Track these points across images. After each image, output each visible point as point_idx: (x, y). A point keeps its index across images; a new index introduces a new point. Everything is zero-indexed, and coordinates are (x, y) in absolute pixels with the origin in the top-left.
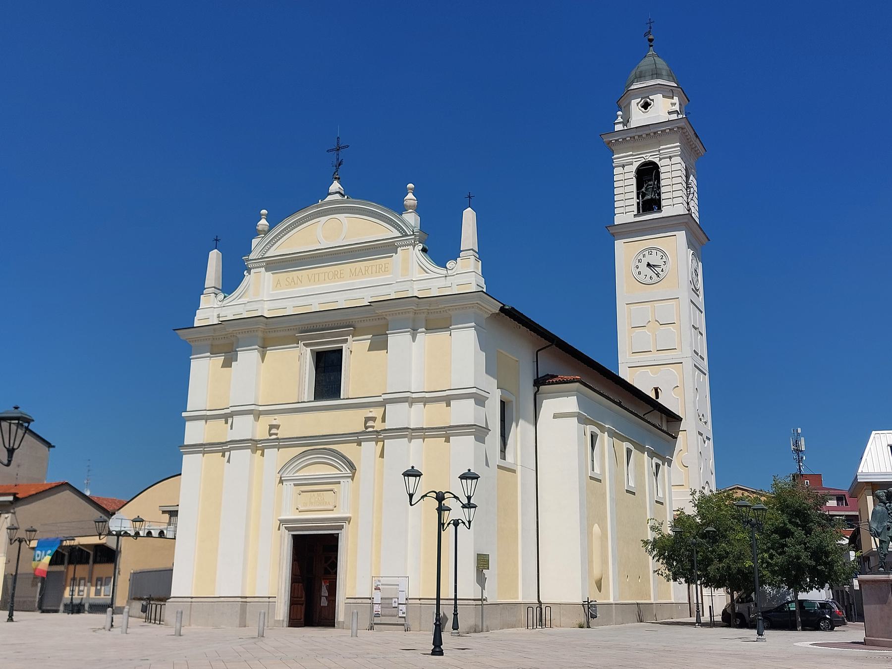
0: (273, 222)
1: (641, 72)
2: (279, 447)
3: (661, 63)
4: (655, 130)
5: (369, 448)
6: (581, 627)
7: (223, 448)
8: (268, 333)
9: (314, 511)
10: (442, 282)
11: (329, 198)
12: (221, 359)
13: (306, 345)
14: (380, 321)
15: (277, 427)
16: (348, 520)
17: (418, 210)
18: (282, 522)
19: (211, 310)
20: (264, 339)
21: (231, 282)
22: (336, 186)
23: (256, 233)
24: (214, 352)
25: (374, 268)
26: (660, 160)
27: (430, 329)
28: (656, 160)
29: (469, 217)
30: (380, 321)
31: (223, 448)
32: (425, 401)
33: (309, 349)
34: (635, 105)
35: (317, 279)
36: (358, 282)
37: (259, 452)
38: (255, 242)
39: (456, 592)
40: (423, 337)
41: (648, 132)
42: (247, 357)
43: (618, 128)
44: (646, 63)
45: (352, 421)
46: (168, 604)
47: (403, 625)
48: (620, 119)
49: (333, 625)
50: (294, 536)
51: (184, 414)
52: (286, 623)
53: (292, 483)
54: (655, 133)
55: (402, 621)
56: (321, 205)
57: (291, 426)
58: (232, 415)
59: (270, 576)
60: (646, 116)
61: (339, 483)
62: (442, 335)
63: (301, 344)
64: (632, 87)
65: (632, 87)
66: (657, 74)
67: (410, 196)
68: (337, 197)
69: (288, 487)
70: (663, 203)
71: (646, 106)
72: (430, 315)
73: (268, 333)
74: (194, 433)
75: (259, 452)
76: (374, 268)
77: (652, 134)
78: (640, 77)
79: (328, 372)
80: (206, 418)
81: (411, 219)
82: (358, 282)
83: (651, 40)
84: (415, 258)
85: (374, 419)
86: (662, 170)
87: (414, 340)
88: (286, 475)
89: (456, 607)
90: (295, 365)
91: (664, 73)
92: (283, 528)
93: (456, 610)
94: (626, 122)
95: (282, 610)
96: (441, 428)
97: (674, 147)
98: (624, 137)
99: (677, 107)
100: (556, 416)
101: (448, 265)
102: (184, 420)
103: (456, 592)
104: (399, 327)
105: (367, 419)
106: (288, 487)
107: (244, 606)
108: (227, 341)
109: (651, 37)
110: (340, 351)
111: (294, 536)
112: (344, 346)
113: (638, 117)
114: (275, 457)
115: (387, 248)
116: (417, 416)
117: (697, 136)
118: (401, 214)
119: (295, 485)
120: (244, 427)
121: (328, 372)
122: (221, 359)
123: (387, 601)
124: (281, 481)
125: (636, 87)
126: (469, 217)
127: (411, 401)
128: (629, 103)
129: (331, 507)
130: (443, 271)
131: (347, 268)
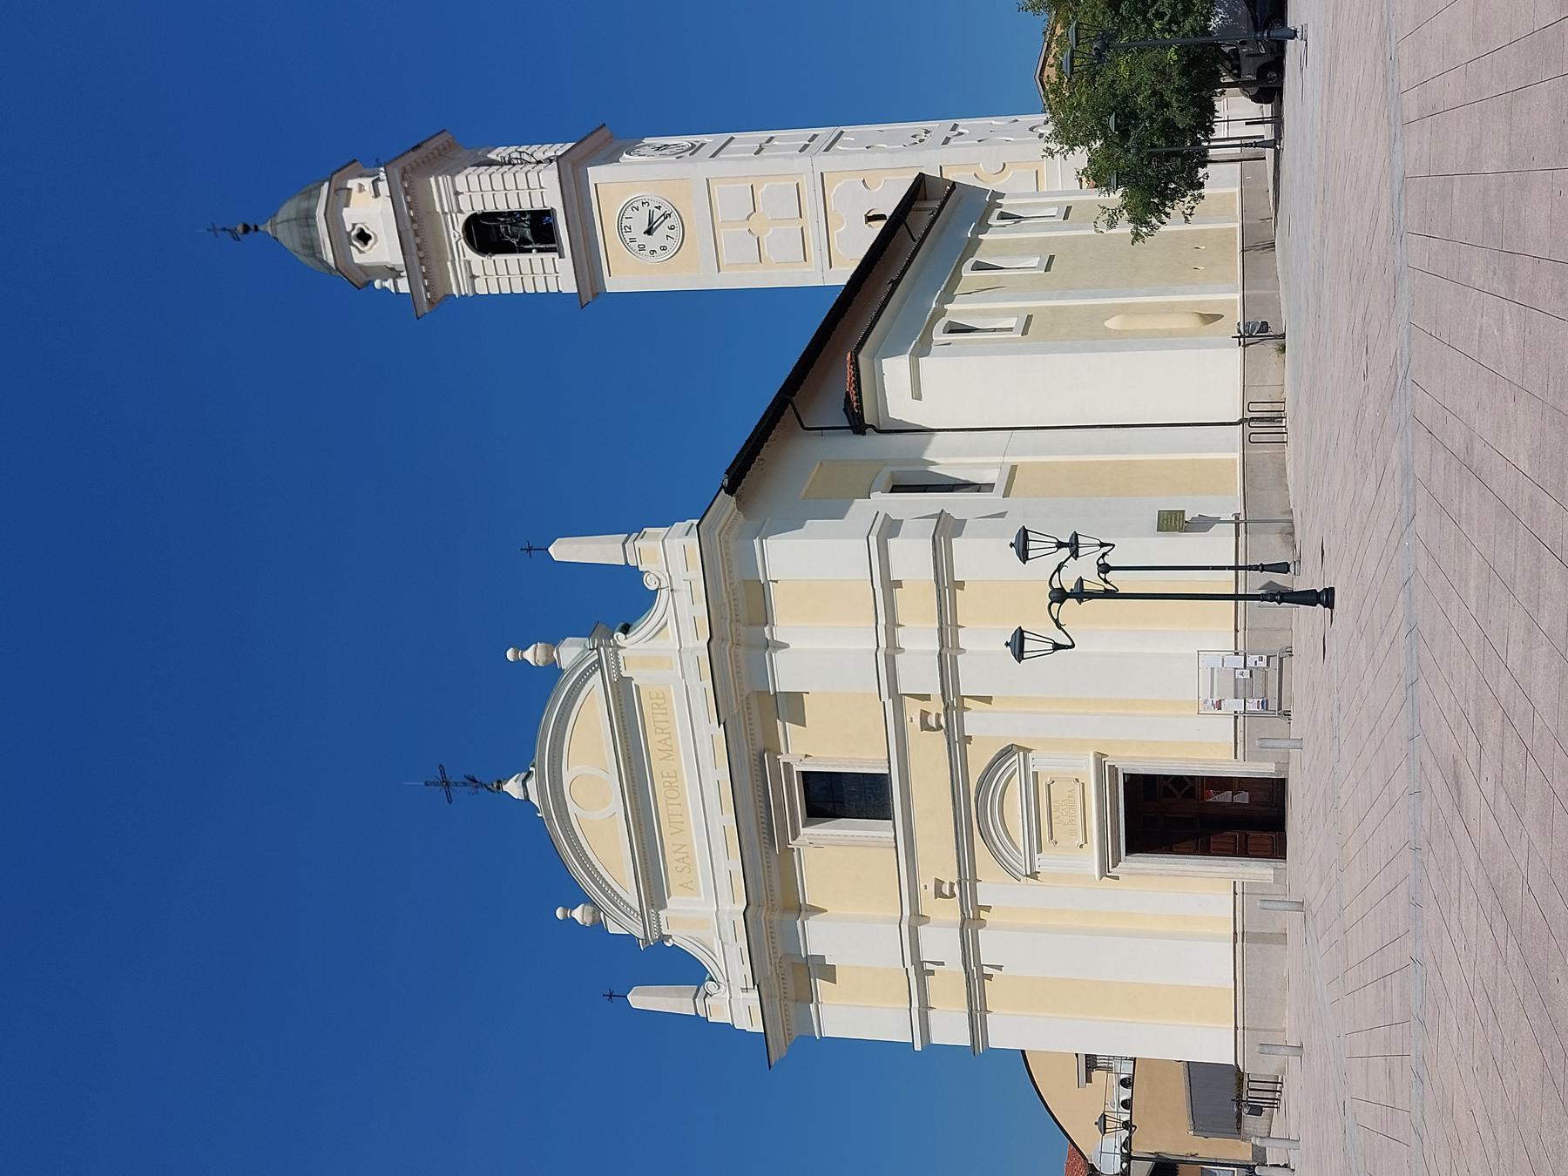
0: (579, 896)
1: (304, 246)
3: (289, 210)
4: (408, 221)
5: (975, 721)
6: (1283, 349)
7: (976, 977)
8: (774, 903)
9: (1085, 817)
10: (683, 597)
11: (534, 798)
12: (821, 985)
13: (795, 835)
14: (752, 707)
15: (939, 884)
16: (1100, 758)
17: (554, 641)
18: (1104, 872)
19: (734, 1003)
20: (785, 909)
21: (684, 969)
22: (512, 788)
23: (598, 927)
24: (808, 996)
25: (659, 718)
26: (460, 211)
27: (766, 618)
28: (462, 218)
29: (565, 550)
30: (752, 707)
31: (976, 977)
32: (893, 624)
33: (803, 831)
34: (363, 256)
35: (679, 819)
36: (683, 745)
37: (983, 914)
38: (613, 929)
39: (1223, 568)
40: (781, 630)
41: (411, 233)
42: (818, 938)
43: (404, 286)
44: (288, 237)
45: (929, 752)
46: (1247, 1069)
47: (1281, 659)
48: (389, 284)
49: (1282, 783)
50: (1128, 852)
51: (918, 1047)
52: (1280, 864)
54: (413, 221)
55: (1275, 662)
56: (547, 812)
57: (937, 860)
58: (918, 963)
59: (1197, 893)
60: (382, 236)
61: (1036, 774)
62: (776, 593)
63: (793, 844)
64: (331, 261)
65: (331, 261)
66: (307, 219)
67: (528, 655)
68: (532, 784)
69: (1042, 862)
70: (538, 206)
71: (364, 237)
72: (741, 616)
73: (774, 903)
74: (950, 1029)
75: (983, 914)
76: (659, 718)
77: (416, 228)
78: (313, 248)
79: (842, 796)
80: (925, 1008)
81: (569, 653)
82: (683, 745)
83: (246, 229)
84: (640, 645)
85: (924, 715)
86: (479, 208)
87: (786, 646)
88: (1023, 868)
89: (1250, 568)
90: (830, 853)
91: (304, 205)
92: (1114, 872)
93: (1256, 568)
94: (394, 273)
95: (1256, 871)
96: (939, 597)
97: (439, 187)
98: (420, 276)
99: (367, 182)
100: (917, 396)
101: (652, 587)
102: (929, 1047)
103: (1223, 568)
104: (762, 672)
105: (925, 726)
106: (1042, 862)
108: (789, 973)
109: (240, 228)
110: (806, 776)
111: (1128, 852)
112: (796, 769)
113: (385, 250)
114: (992, 887)
115: (623, 696)
116: (919, 640)
117: (418, 146)
118: (562, 671)
120: (941, 942)
121: (842, 796)
122: (821, 985)
123: (1240, 688)
124: (1034, 875)
125: (331, 256)
126: (565, 550)
127: (893, 649)
128: (360, 267)
129: (1078, 787)
130: (663, 596)
131: (658, 766)
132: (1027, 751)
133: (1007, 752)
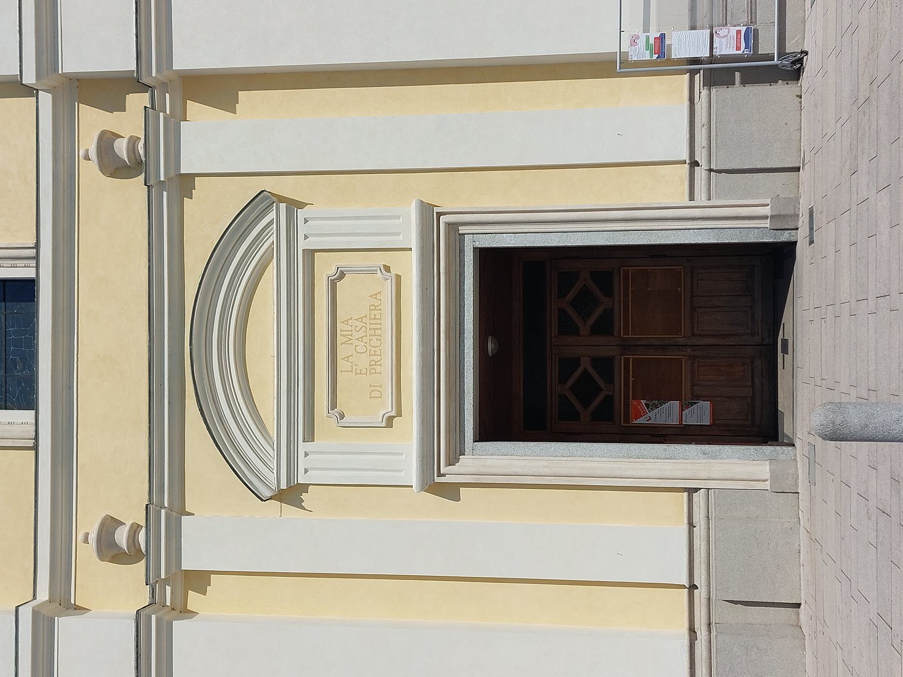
2: (180, 510)
9: (397, 341)
15: (109, 525)
16: (429, 214)
37: (194, 600)
53: (303, 447)
59: (618, 512)
69: (317, 462)
75: (194, 600)
85: (106, 141)
88: (272, 476)
89: (719, 171)
95: (735, 466)
105: (114, 167)
106: (317, 462)
107: (734, 612)
114: (219, 526)
119: (310, 436)
124: (291, 494)
132: (294, 205)
133: (262, 202)
